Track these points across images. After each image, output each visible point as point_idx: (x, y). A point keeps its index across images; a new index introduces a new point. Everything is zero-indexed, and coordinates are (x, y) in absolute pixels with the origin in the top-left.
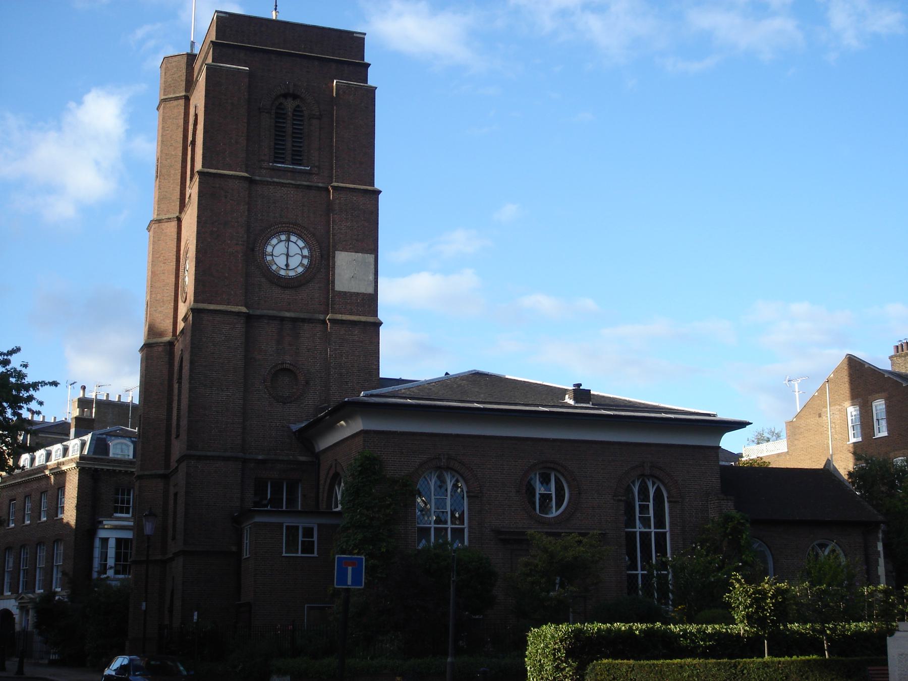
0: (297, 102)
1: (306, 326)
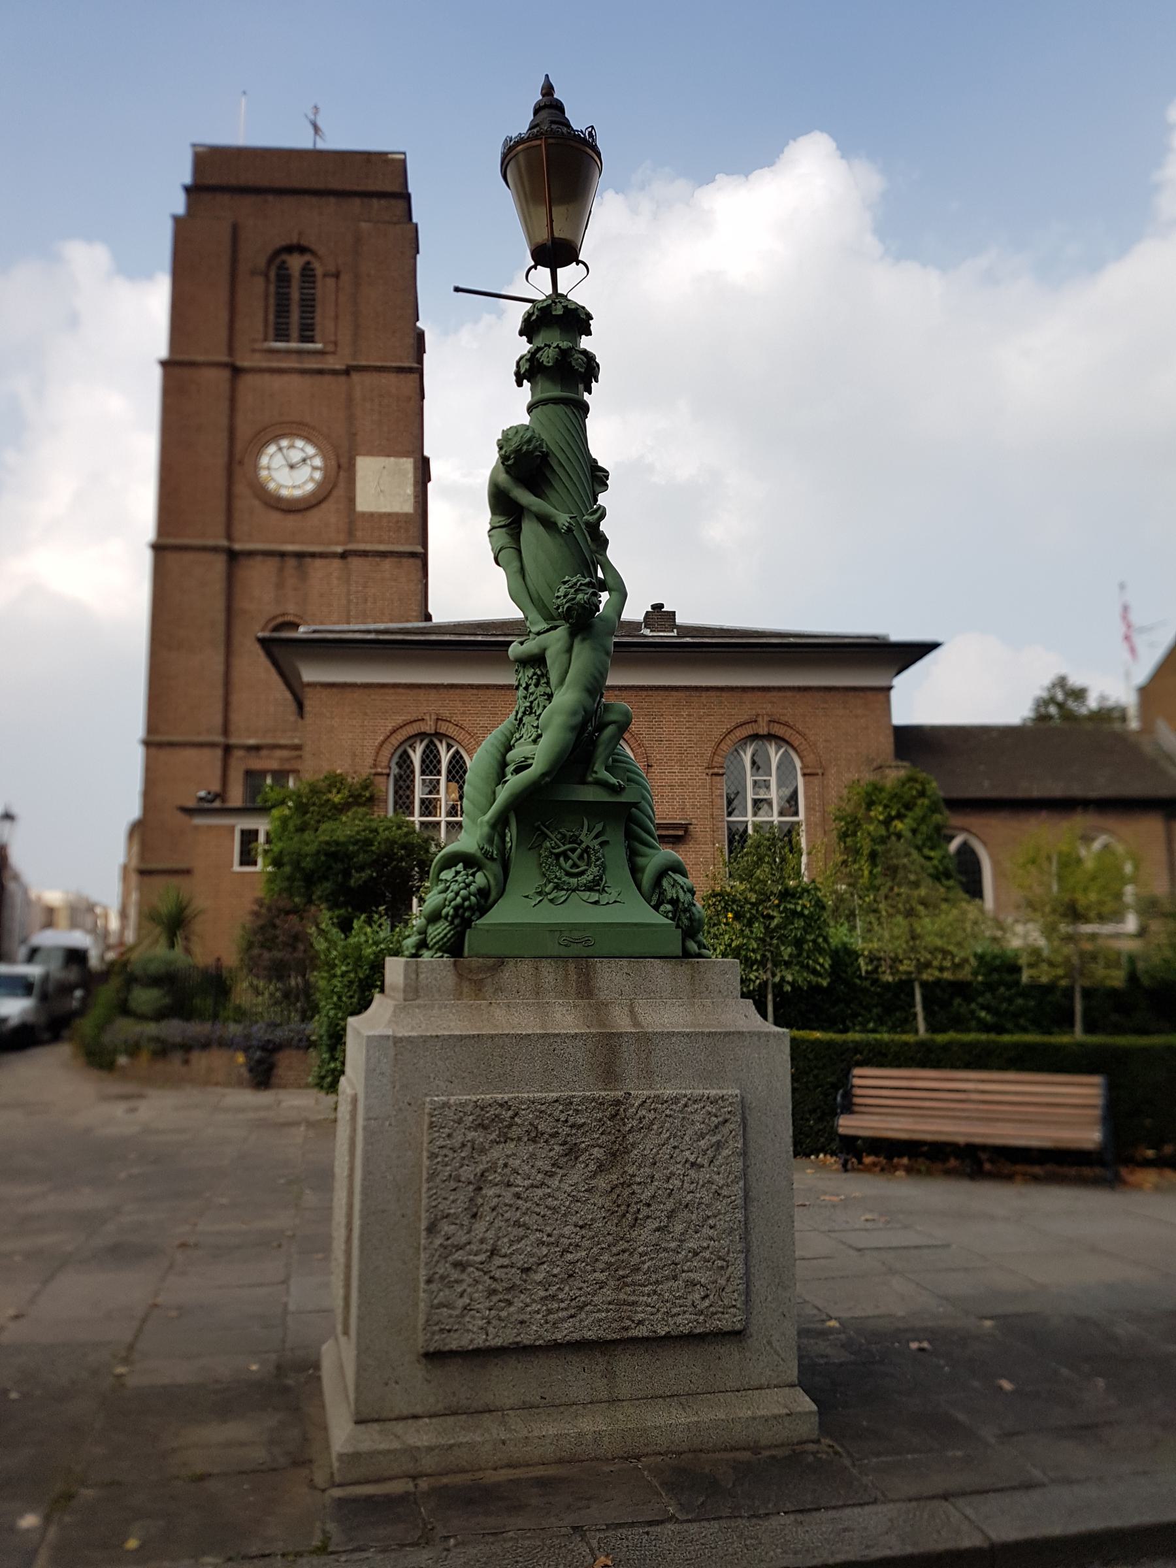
0: (307, 257)
1: (318, 562)
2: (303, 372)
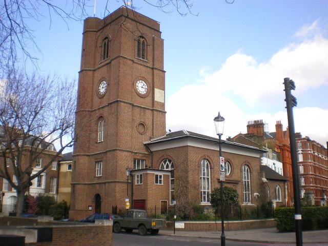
1: (147, 111)
2: (145, 66)
